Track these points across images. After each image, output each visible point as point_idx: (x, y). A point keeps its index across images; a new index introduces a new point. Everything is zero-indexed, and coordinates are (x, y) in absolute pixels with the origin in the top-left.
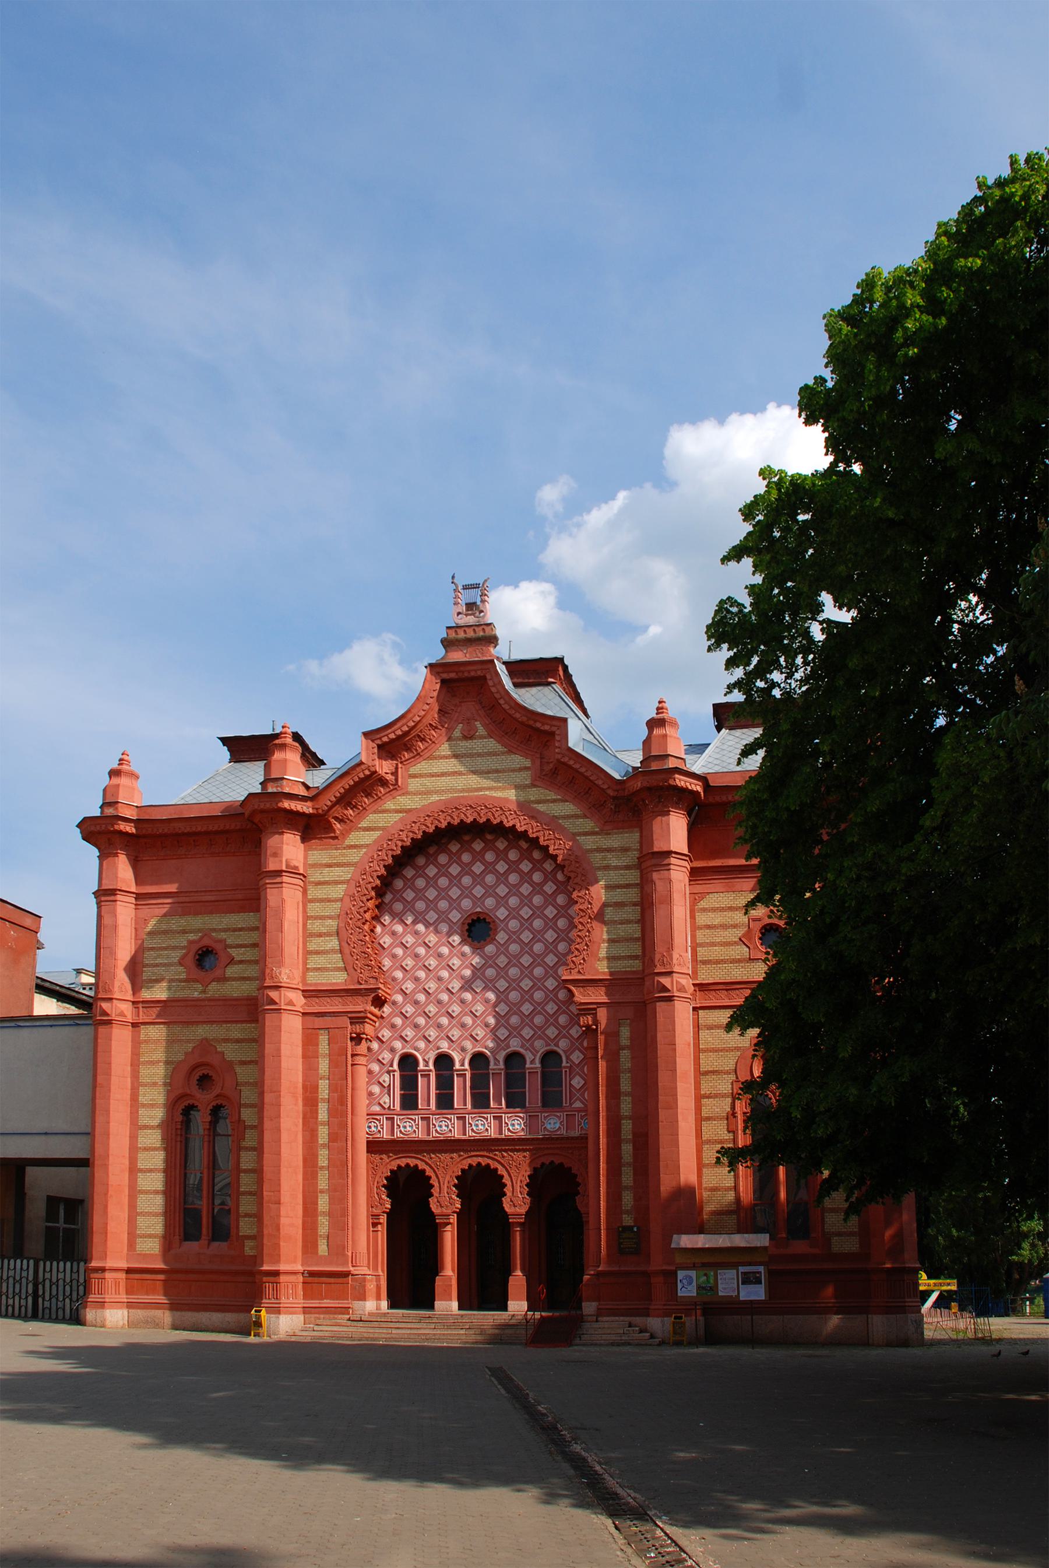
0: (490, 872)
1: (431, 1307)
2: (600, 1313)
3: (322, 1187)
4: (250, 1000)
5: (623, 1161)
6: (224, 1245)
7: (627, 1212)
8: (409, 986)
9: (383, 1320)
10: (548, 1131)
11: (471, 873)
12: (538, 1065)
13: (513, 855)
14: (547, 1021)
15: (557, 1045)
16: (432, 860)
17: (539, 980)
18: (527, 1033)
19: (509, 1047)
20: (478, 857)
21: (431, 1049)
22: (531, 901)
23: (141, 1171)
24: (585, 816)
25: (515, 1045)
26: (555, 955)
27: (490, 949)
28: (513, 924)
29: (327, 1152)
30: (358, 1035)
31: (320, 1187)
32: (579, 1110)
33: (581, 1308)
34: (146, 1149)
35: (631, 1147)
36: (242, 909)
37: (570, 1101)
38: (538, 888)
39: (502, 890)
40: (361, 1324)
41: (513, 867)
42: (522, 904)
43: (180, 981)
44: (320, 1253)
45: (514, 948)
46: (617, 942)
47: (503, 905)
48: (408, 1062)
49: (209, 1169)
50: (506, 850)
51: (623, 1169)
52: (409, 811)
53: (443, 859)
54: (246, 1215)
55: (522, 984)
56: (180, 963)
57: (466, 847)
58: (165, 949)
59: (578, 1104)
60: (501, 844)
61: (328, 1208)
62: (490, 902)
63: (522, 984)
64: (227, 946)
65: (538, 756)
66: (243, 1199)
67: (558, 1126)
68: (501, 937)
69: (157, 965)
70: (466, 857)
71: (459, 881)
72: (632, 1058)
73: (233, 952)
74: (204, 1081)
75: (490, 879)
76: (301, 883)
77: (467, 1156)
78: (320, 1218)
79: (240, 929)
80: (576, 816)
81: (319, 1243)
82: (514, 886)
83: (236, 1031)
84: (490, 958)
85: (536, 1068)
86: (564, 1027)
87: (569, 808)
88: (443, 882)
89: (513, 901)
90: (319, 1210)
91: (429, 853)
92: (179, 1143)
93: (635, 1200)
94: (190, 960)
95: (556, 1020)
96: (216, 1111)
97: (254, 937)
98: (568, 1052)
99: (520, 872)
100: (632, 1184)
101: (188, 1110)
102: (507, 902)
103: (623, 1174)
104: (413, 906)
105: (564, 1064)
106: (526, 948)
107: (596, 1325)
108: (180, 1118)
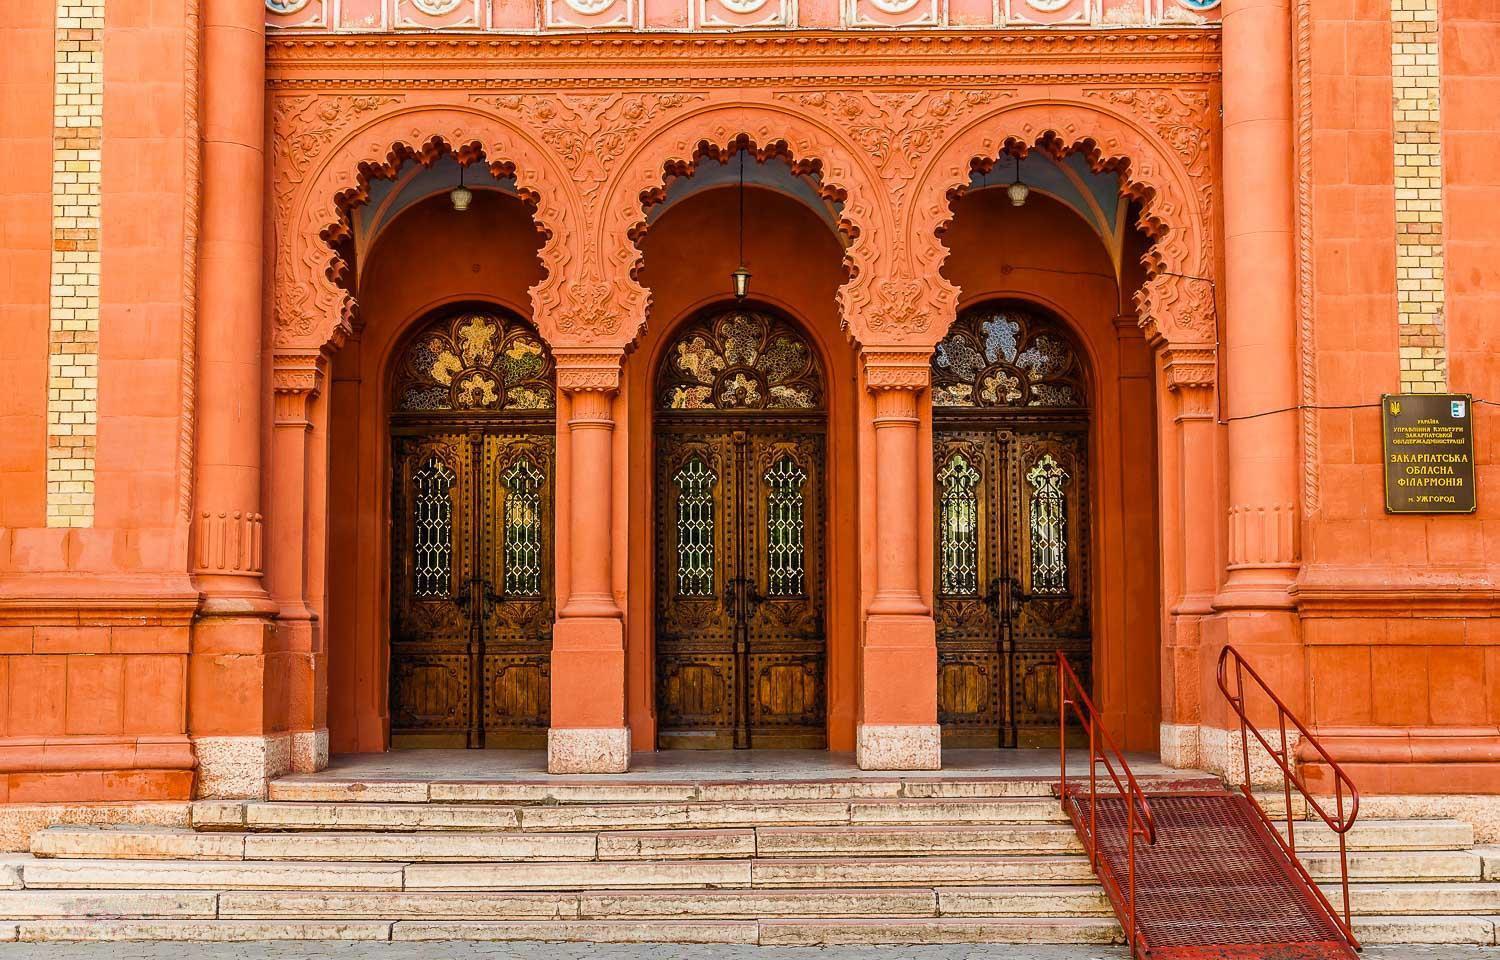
1: (543, 746)
3: (71, 223)
5: (1398, 116)
7: (1423, 338)
9: (347, 817)
29: (97, 68)
31: (59, 223)
35: (1434, 60)
40: (232, 844)
44: (55, 519)
51: (1398, 149)
61: (94, 314)
77: (696, 105)
78: (55, 360)
81: (51, 476)
90: (56, 326)
93: (1456, 287)
100: (1437, 217)
103: (1399, 172)
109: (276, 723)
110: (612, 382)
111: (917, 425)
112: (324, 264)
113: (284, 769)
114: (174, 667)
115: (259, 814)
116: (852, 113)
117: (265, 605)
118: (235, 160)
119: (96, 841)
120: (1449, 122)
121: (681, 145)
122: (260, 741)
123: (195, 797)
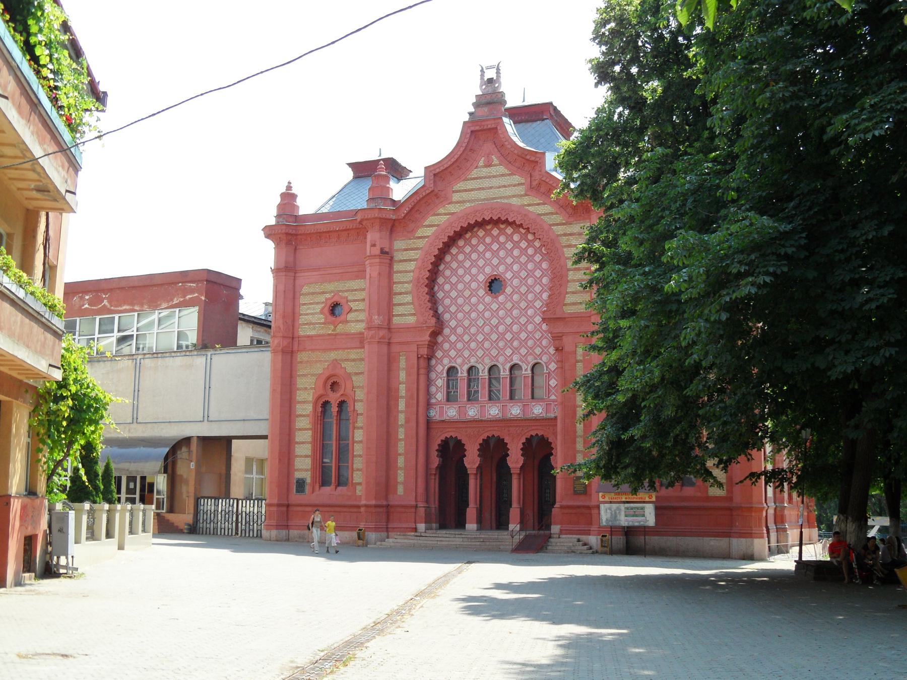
0: (503, 249)
2: (562, 532)
4: (361, 334)
6: (344, 488)
8: (453, 323)
10: (535, 414)
11: (490, 250)
12: (529, 372)
13: (516, 237)
14: (535, 343)
15: (541, 359)
16: (468, 242)
17: (531, 317)
18: (523, 351)
19: (512, 360)
20: (495, 239)
21: (466, 363)
22: (526, 266)
23: (298, 443)
24: (557, 213)
25: (516, 359)
26: (541, 301)
27: (501, 298)
28: (516, 282)
30: (422, 356)
32: (554, 401)
33: (550, 529)
34: (300, 430)
36: (357, 277)
37: (549, 394)
38: (530, 258)
39: (509, 260)
40: (418, 538)
41: (516, 245)
42: (521, 269)
43: (320, 323)
44: (399, 493)
45: (516, 297)
46: (575, 293)
47: (510, 270)
48: (451, 370)
49: (336, 441)
50: (512, 234)
52: (452, 214)
53: (474, 241)
54: (358, 470)
55: (521, 320)
56: (322, 312)
57: (488, 233)
58: (311, 304)
59: (553, 397)
60: (509, 230)
62: (502, 268)
63: (521, 320)
64: (348, 301)
65: (529, 176)
66: (356, 460)
67: (541, 411)
68: (508, 290)
69: (307, 314)
70: (488, 240)
71: (484, 255)
72: (584, 368)
73: (352, 305)
74: (334, 386)
75: (502, 253)
76: (388, 261)
79: (356, 290)
80: (552, 214)
82: (517, 257)
83: (353, 354)
84: (502, 303)
85: (528, 374)
86: (545, 347)
87: (547, 208)
88: (474, 256)
89: (516, 267)
91: (466, 239)
92: (319, 425)
94: (326, 310)
95: (541, 343)
96: (341, 404)
97: (363, 295)
98: (547, 364)
99: (519, 248)
101: (326, 404)
102: (512, 268)
104: (457, 272)
105: (545, 371)
106: (523, 296)
107: (558, 540)
108: (320, 409)
109: (428, 521)
110: (475, 472)
111: (520, 479)
112: (436, 455)
113: (427, 529)
114: (414, 514)
115: (422, 534)
116: (509, 431)
117: (427, 506)
118: (422, 442)
119: (402, 537)
120: (584, 435)
121: (485, 436)
122: (424, 525)
123: (416, 532)
